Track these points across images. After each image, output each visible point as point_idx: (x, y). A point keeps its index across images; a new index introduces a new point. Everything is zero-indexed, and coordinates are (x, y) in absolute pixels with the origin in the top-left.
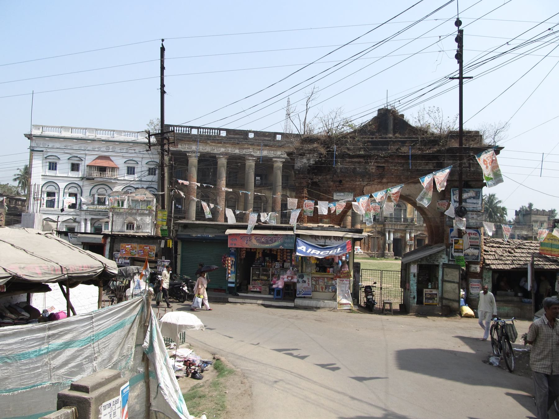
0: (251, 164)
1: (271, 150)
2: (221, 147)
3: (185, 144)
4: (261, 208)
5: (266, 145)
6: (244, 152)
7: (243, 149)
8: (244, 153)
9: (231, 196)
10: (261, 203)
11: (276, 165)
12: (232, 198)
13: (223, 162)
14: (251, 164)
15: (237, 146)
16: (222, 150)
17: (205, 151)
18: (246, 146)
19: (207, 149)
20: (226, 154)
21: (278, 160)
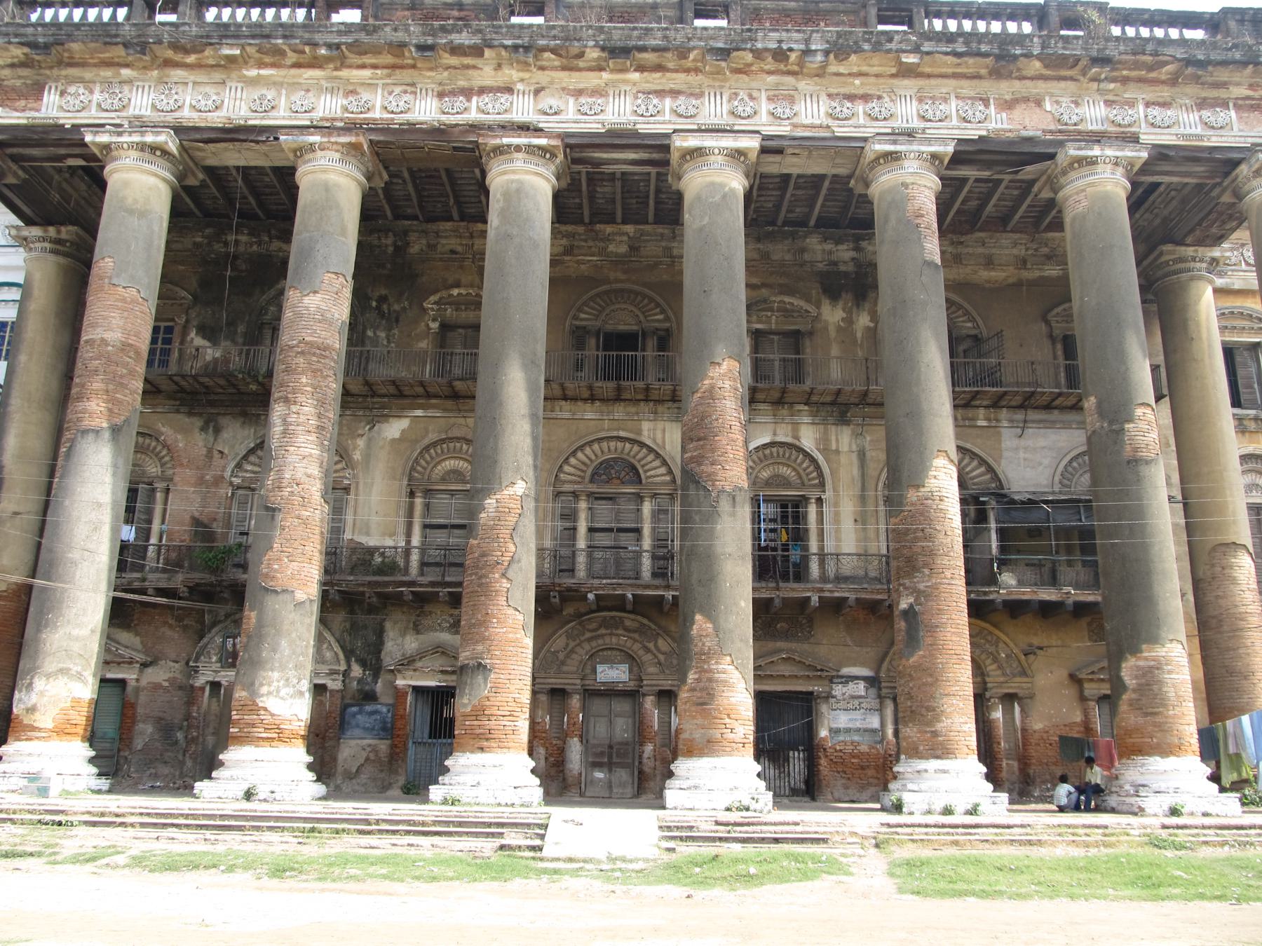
0: (524, 188)
1: (660, 93)
2: (321, 90)
3: (88, 85)
4: (638, 531)
5: (618, 53)
6: (474, 111)
7: (468, 93)
8: (473, 116)
9: (449, 464)
10: (639, 498)
11: (694, 182)
12: (457, 475)
13: (333, 188)
14: (524, 188)
15: (430, 79)
16: (329, 106)
17: (217, 119)
18: (486, 74)
19: (231, 102)
20: (352, 127)
21: (708, 142)
